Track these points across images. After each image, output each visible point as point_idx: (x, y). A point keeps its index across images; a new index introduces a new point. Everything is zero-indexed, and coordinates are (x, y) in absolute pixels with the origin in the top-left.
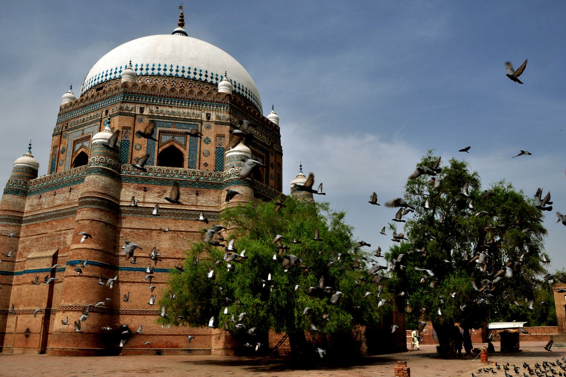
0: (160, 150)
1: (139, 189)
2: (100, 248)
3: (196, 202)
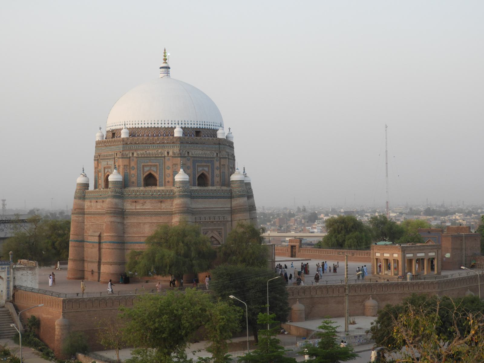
0: (144, 176)
1: (133, 202)
2: (116, 235)
3: (161, 207)
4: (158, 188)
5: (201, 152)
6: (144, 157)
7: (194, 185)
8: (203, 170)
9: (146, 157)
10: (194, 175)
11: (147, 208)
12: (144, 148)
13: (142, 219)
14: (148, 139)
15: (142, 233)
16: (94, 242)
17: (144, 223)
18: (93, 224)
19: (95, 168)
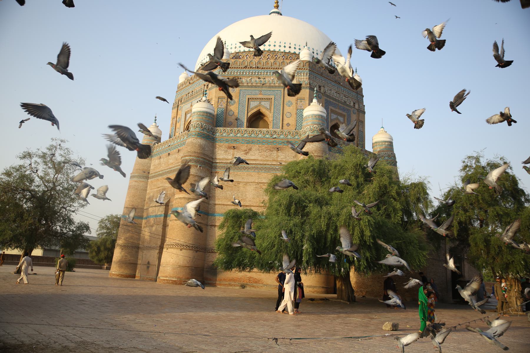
0: (249, 114)
1: (229, 148)
6: (252, 86)
8: (337, 119)
9: (256, 87)
11: (253, 158)
17: (246, 183)
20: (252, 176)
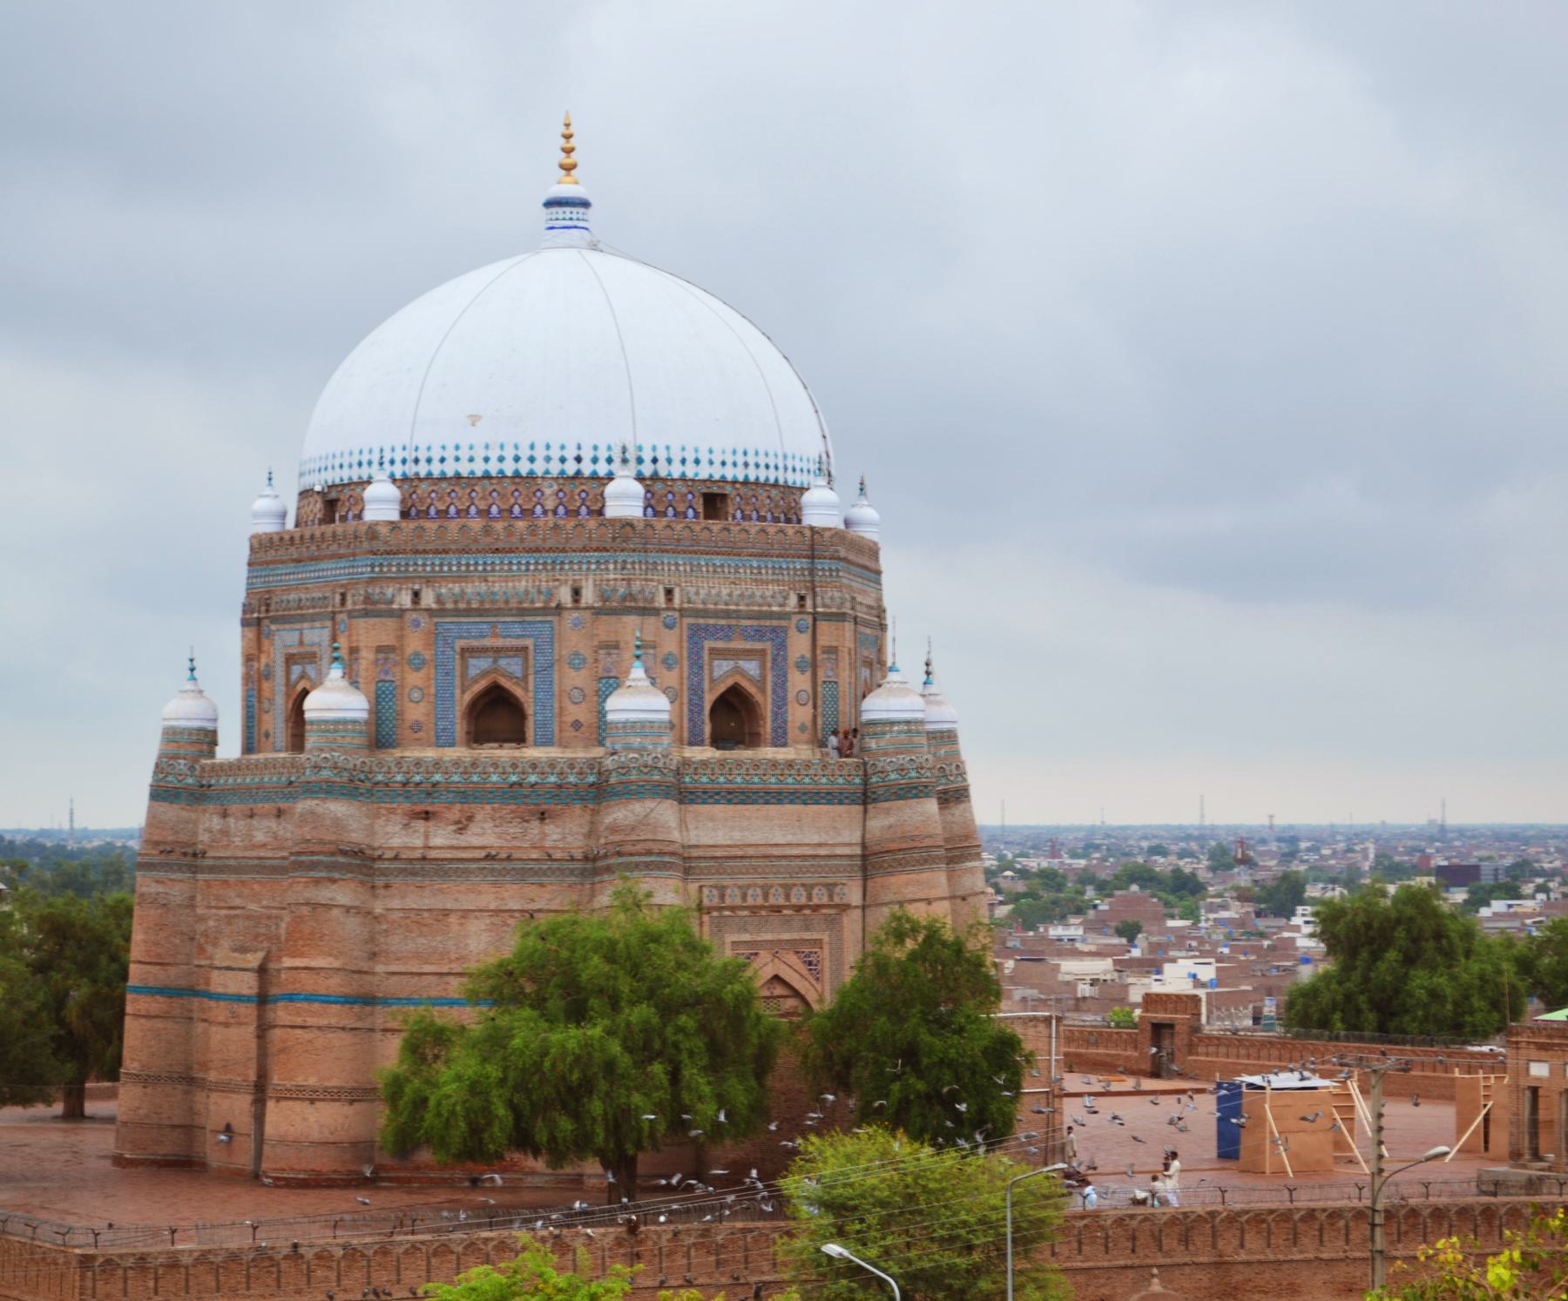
0: (468, 697)
3: (542, 839)
4: (531, 753)
5: (725, 592)
6: (468, 612)
7: (695, 741)
8: (738, 671)
10: (696, 691)
11: (476, 841)
12: (468, 570)
13: (457, 896)
14: (487, 531)
15: (453, 956)
16: (239, 998)
17: (465, 914)
18: (236, 916)
19: (248, 659)
20: (480, 893)
